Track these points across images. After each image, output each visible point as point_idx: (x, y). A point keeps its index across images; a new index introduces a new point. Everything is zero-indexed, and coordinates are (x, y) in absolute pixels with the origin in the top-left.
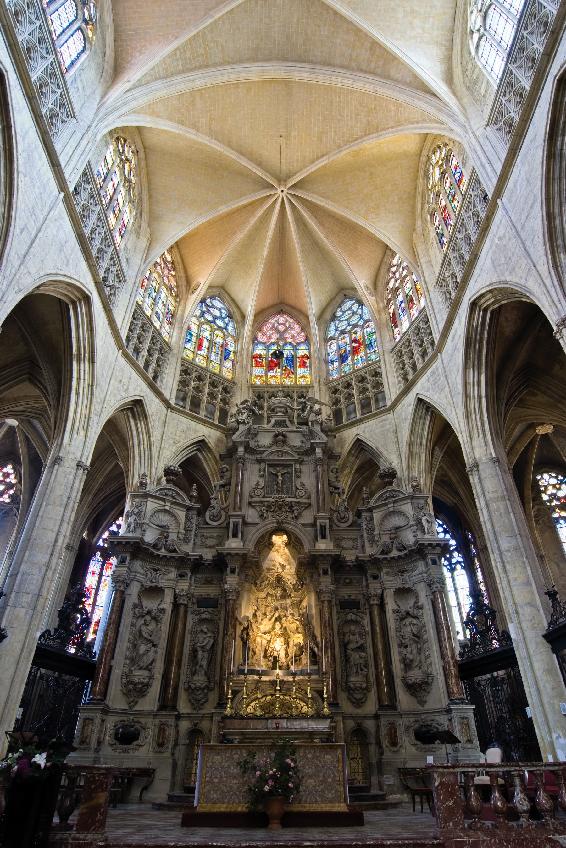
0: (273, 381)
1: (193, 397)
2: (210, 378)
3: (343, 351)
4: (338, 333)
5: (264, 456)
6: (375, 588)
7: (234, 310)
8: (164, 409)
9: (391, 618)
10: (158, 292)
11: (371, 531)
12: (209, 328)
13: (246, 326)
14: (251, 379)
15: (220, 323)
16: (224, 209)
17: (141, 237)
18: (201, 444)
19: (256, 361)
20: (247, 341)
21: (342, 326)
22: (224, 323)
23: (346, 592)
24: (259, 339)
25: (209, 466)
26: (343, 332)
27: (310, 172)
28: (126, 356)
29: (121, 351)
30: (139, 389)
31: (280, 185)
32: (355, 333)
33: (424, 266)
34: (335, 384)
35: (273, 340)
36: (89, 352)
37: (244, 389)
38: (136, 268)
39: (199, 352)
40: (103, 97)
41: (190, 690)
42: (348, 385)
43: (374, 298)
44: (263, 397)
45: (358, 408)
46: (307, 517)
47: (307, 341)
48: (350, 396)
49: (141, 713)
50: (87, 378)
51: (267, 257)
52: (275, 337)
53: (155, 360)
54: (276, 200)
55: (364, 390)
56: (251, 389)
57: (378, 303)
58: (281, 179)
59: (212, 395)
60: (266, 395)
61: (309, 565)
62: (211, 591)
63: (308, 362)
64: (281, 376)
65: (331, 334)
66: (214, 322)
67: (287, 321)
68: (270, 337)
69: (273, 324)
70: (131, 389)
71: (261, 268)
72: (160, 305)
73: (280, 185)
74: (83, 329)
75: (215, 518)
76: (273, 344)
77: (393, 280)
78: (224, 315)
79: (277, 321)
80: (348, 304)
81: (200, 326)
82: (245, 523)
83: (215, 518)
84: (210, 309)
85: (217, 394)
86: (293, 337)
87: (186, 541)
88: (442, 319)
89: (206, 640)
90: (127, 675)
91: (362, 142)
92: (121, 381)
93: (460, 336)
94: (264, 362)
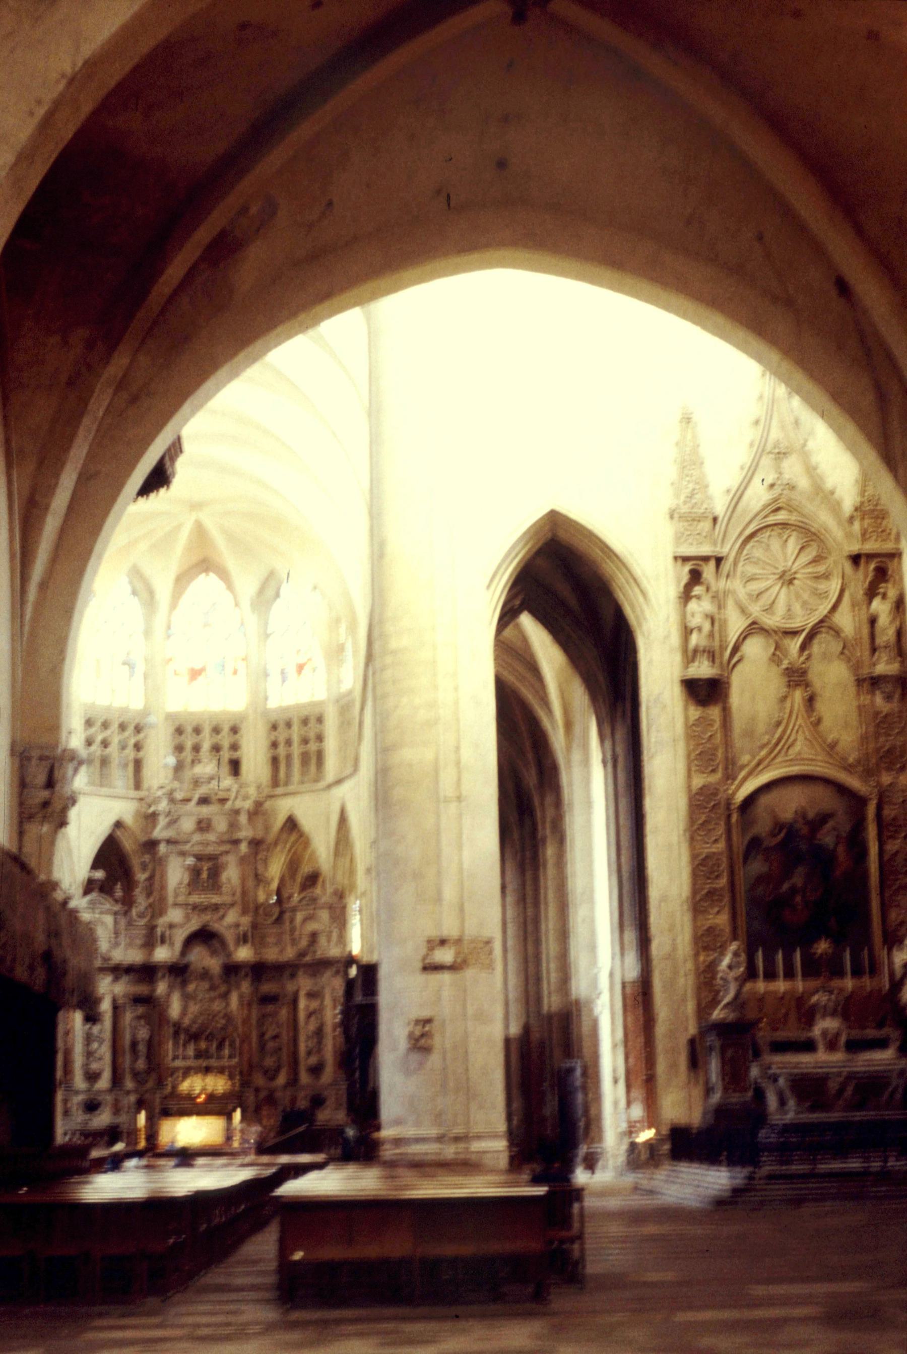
5: (187, 847)
6: (290, 987)
7: (139, 586)
9: (302, 1015)
11: (293, 930)
18: (118, 824)
23: (267, 988)
25: (128, 845)
41: (135, 1075)
42: (289, 725)
46: (232, 917)
48: (289, 743)
49: (100, 1092)
55: (305, 741)
60: (189, 729)
62: (142, 989)
75: (141, 916)
82: (171, 926)
83: (141, 916)
87: (117, 945)
89: (143, 1033)
90: (86, 1066)
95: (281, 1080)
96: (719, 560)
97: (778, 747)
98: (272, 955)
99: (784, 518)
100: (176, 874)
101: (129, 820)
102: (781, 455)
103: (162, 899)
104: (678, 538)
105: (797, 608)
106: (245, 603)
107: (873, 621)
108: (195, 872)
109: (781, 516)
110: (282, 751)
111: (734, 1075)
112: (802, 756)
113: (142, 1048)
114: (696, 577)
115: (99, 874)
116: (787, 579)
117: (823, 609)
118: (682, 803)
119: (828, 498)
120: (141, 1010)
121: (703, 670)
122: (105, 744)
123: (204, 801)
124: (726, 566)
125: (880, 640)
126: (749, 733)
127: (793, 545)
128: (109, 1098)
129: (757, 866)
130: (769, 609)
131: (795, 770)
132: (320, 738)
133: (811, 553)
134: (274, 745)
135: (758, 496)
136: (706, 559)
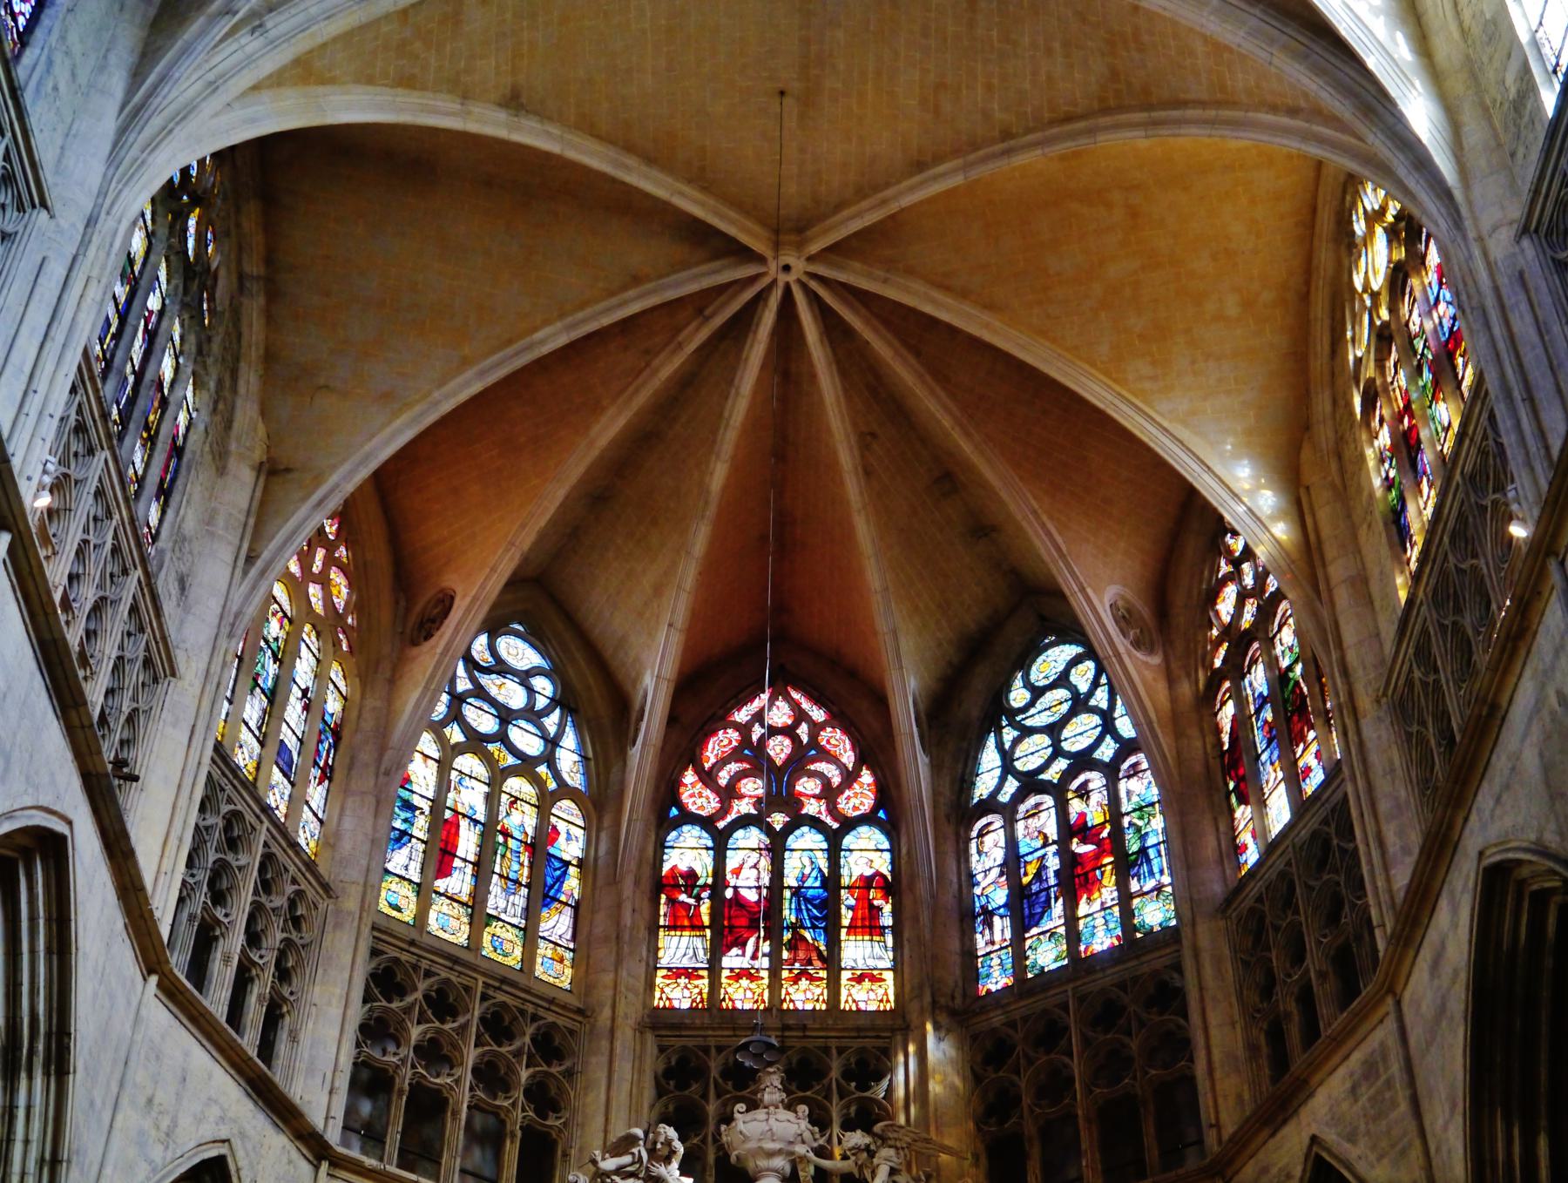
0: (742, 996)
1: (417, 1088)
2: (484, 997)
3: (1032, 869)
4: (1012, 785)
8: (305, 1168)
10: (285, 657)
12: (481, 770)
13: (635, 753)
14: (650, 986)
16: (552, 338)
17: (232, 463)
19: (672, 901)
20: (638, 826)
21: (1032, 754)
22: (544, 736)
24: (685, 798)
26: (1031, 783)
27: (893, 207)
28: (171, 992)
29: (154, 979)
30: (215, 1111)
31: (777, 246)
32: (1084, 793)
33: (1342, 597)
34: (997, 1019)
35: (744, 807)
36: (48, 1035)
37: (625, 1035)
38: (215, 606)
39: (441, 884)
40: (137, 75)
42: (1051, 1034)
43: (1156, 660)
44: (701, 1073)
45: (1087, 1140)
48: (1056, 1085)
50: (35, 1135)
51: (725, 488)
52: (753, 787)
53: (270, 958)
54: (761, 297)
56: (650, 1037)
57: (1171, 681)
58: (789, 228)
59: (491, 1076)
60: (715, 1066)
63: (887, 908)
64: (774, 972)
65: (984, 786)
66: (502, 737)
67: (800, 716)
68: (729, 794)
69: (745, 729)
70: (185, 1121)
71: (700, 538)
72: (294, 711)
73: (777, 246)
74: (33, 951)
76: (744, 822)
77: (1230, 591)
78: (541, 703)
79: (759, 717)
80: (1056, 657)
81: (444, 766)
84: (485, 680)
85: (511, 1070)
86: (829, 794)
88: (1406, 850)
91: (1091, 132)
92: (150, 1101)
93: (1456, 973)
94: (705, 909)
122: (434, 1053)
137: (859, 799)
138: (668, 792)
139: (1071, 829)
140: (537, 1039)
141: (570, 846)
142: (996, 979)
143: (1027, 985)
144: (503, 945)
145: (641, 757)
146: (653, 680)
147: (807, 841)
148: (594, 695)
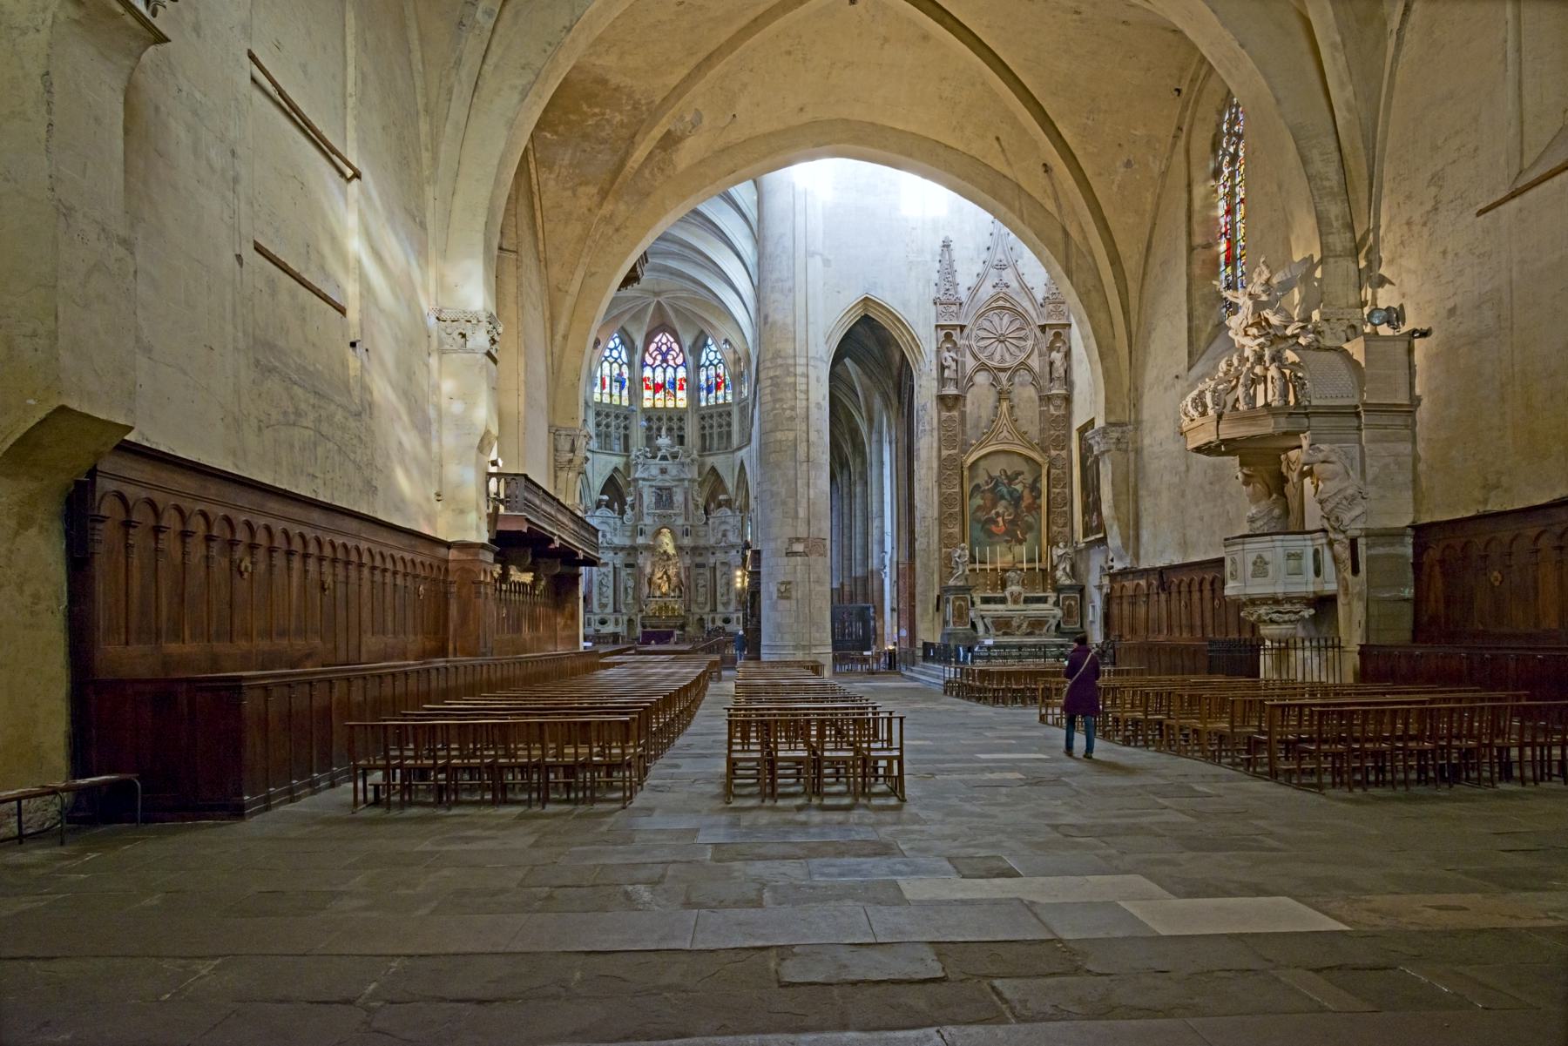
0: (659, 404)
15: (615, 354)
18: (616, 469)
23: (699, 560)
25: (621, 481)
47: (684, 364)
48: (711, 427)
61: (679, 548)
89: (631, 583)
95: (708, 609)
96: (962, 328)
97: (991, 431)
98: (702, 542)
99: (1003, 304)
100: (648, 498)
101: (621, 467)
102: (1001, 267)
103: (641, 512)
104: (938, 316)
105: (1007, 356)
106: (686, 350)
107: (1051, 364)
108: (659, 497)
109: (1001, 303)
110: (707, 432)
111: (960, 614)
112: (1005, 439)
113: (630, 591)
114: (948, 337)
115: (606, 497)
116: (1001, 340)
117: (1023, 356)
118: (935, 465)
119: (1027, 291)
120: (629, 570)
121: (951, 390)
122: (608, 426)
123: (664, 458)
124: (966, 331)
125: (1055, 375)
126: (977, 426)
127: (1006, 319)
128: (612, 618)
129: (978, 501)
130: (990, 357)
131: (1000, 447)
132: (729, 425)
133: (1017, 324)
134: (703, 428)
135: (987, 291)
136: (954, 327)
137: (680, 360)
138: (643, 360)
139: (717, 376)
140: (625, 415)
141: (626, 376)
142: (703, 404)
143: (708, 407)
144: (616, 401)
145: (637, 358)
146: (639, 343)
147: (670, 371)
148: (627, 342)
